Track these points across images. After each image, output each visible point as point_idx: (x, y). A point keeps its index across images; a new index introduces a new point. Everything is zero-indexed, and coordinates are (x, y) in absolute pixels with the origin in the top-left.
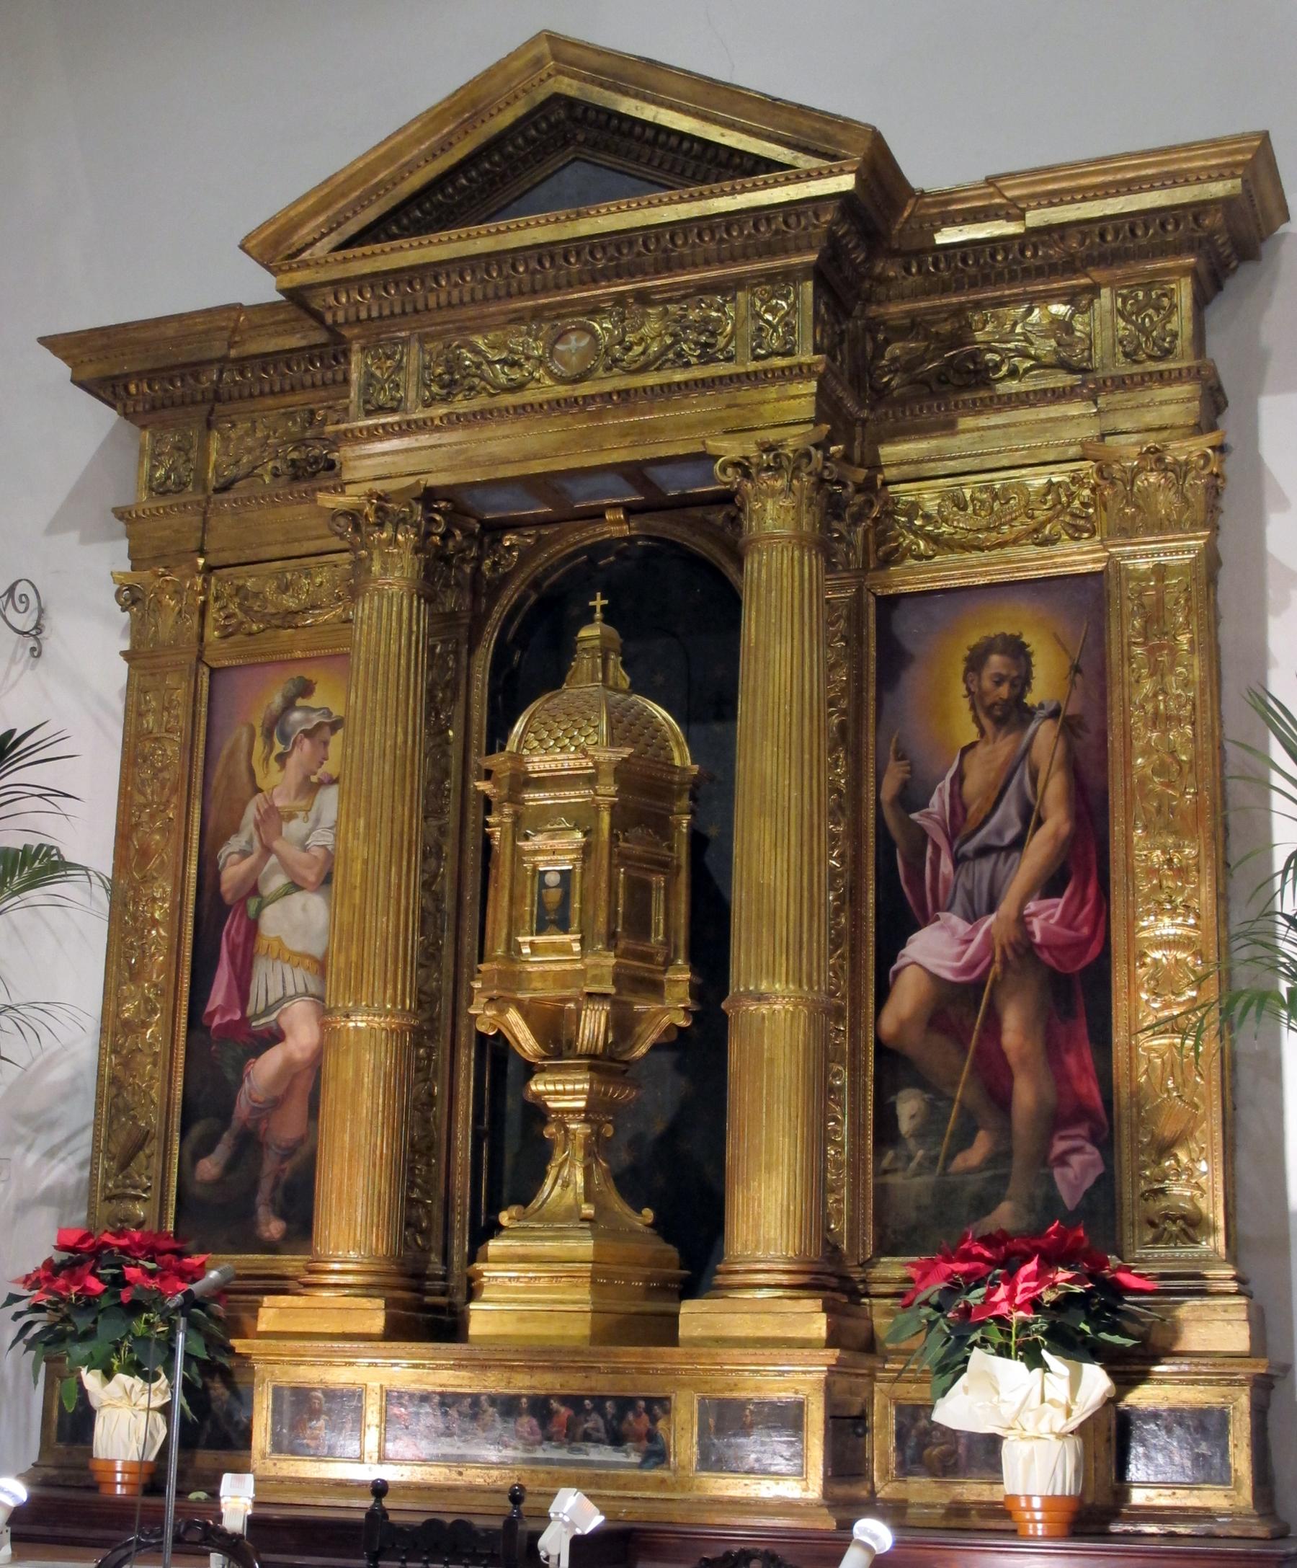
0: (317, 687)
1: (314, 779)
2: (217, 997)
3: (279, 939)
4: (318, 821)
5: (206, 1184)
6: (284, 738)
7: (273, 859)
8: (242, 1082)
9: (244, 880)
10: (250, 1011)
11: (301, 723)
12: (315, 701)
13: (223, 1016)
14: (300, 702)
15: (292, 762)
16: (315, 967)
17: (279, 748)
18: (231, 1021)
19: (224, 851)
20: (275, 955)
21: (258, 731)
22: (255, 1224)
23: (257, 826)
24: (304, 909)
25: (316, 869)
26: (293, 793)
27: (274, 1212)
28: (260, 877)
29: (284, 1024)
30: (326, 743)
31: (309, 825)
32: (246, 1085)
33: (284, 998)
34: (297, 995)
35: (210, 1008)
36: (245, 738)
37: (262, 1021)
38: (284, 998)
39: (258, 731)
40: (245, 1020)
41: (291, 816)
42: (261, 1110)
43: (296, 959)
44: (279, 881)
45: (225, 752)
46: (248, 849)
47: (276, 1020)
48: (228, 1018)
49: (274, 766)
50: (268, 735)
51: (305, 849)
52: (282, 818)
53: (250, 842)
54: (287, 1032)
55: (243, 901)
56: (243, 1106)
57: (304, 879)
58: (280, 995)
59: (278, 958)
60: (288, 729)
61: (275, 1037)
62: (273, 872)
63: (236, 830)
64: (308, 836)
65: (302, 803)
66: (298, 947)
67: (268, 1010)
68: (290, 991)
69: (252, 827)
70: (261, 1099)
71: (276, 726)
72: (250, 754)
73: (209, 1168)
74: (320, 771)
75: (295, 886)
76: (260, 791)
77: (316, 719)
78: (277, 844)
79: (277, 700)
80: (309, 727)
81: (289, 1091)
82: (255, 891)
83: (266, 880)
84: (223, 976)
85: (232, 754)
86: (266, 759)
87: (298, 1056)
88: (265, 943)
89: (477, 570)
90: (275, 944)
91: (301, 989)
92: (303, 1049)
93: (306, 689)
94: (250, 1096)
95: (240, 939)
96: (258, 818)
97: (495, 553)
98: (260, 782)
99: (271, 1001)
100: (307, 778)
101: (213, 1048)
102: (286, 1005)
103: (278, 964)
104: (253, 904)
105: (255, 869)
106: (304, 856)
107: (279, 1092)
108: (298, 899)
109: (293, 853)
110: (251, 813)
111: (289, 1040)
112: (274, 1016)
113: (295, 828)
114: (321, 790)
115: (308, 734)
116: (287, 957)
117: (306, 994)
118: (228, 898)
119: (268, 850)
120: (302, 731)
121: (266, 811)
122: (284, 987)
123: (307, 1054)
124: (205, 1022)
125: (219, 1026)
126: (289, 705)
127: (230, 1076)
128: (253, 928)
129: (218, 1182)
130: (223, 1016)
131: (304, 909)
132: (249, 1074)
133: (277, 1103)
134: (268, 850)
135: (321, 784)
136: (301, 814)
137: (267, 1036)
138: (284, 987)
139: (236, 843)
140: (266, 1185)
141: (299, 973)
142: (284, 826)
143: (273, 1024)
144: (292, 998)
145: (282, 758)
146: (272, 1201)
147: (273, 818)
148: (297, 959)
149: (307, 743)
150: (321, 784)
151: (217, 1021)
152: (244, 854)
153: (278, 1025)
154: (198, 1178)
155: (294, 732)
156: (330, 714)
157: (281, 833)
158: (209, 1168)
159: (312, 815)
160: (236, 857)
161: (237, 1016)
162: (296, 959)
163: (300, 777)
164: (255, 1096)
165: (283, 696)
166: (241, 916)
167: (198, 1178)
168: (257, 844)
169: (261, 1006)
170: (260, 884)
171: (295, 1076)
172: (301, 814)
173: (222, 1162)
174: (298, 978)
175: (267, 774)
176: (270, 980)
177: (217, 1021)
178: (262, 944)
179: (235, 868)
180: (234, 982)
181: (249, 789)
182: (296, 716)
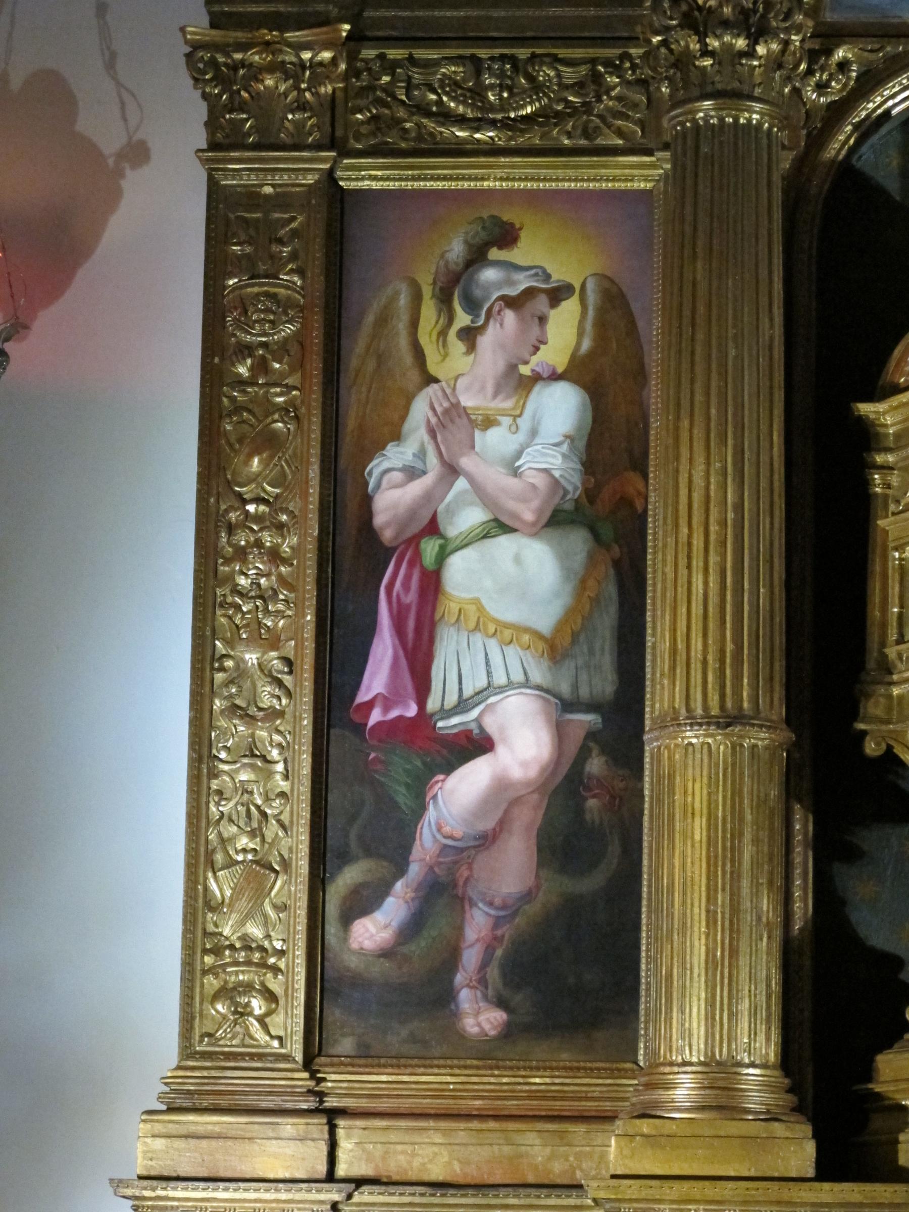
0: (523, 234)
1: (525, 370)
2: (376, 679)
3: (477, 602)
4: (534, 433)
5: (361, 953)
6: (472, 306)
7: (461, 484)
8: (423, 808)
9: (413, 513)
10: (432, 704)
11: (499, 285)
12: (517, 255)
13: (386, 709)
14: (494, 254)
15: (485, 341)
16: (541, 645)
17: (462, 319)
18: (400, 718)
19: (376, 467)
20: (472, 625)
21: (427, 292)
22: (456, 1015)
23: (432, 433)
24: (518, 559)
25: (536, 503)
26: (490, 389)
27: (485, 997)
28: (441, 508)
29: (491, 725)
30: (543, 320)
31: (521, 437)
32: (431, 814)
33: (490, 689)
34: (510, 685)
35: (363, 697)
36: (403, 301)
37: (455, 720)
38: (490, 689)
39: (427, 292)
40: (424, 719)
41: (489, 423)
42: (462, 850)
43: (507, 633)
44: (472, 517)
45: (370, 318)
46: (419, 465)
47: (477, 720)
48: (394, 714)
49: (457, 347)
50: (444, 299)
51: (516, 472)
52: (473, 424)
53: (421, 454)
54: (495, 736)
55: (414, 541)
56: (426, 842)
57: (516, 516)
58: (482, 682)
59: (477, 628)
60: (478, 293)
61: (476, 744)
62: (461, 502)
63: (397, 436)
64: (519, 455)
65: (508, 404)
66: (509, 616)
67: (463, 706)
68: (500, 679)
69: (422, 434)
70: (458, 833)
71: (455, 286)
72: (414, 324)
73: (372, 932)
74: (534, 359)
75: (500, 526)
76: (437, 381)
77: (523, 282)
78: (466, 462)
79: (456, 250)
80: (513, 292)
81: (503, 825)
82: (433, 528)
83: (451, 512)
84: (383, 651)
85: (383, 320)
86: (443, 334)
87: (517, 773)
88: (454, 607)
89: (796, 91)
90: (472, 609)
91: (518, 676)
92: (524, 764)
93: (506, 236)
94: (439, 829)
95: (411, 598)
96: (434, 420)
97: (823, 69)
98: (433, 368)
99: (468, 692)
100: (512, 368)
101: (372, 755)
102: (492, 700)
103: (478, 639)
104: (430, 548)
105: (429, 497)
106: (512, 483)
107: (488, 824)
108: (505, 544)
109: (496, 478)
110: (420, 410)
111: (500, 749)
112: (475, 713)
113: (496, 441)
114: (537, 388)
115: (511, 302)
116: (492, 628)
117: (527, 684)
118: (387, 535)
119: (452, 471)
120: (503, 298)
121: (446, 412)
122: (489, 674)
123: (533, 772)
124: (356, 718)
125: (379, 724)
126: (477, 257)
127: (403, 797)
128: (432, 583)
129: (386, 953)
130: (386, 709)
131: (518, 559)
132: (435, 797)
133: (486, 841)
134: (452, 471)
135: (536, 378)
136: (506, 421)
137: (464, 742)
138: (489, 674)
139: (395, 456)
140: (471, 958)
141: (513, 653)
142: (477, 433)
143: (473, 726)
144: (501, 689)
145: (470, 336)
146: (483, 982)
147: (455, 422)
148: (510, 633)
149: (509, 316)
150: (536, 378)
151: (376, 716)
152: (412, 473)
153: (481, 728)
154: (354, 945)
155: (486, 298)
156: (547, 277)
157: (473, 447)
158: (372, 932)
159: (524, 423)
160: (397, 476)
161: (412, 711)
162: (507, 633)
163: (501, 365)
164: (447, 829)
165: (466, 242)
166: (411, 564)
167: (354, 945)
168: (432, 460)
169: (452, 699)
170: (440, 519)
171: (515, 802)
172: (506, 421)
173: (395, 924)
174: (511, 662)
175: (445, 356)
176: (461, 663)
177: (376, 716)
178: (448, 607)
179: (396, 494)
180: (403, 662)
181: (414, 376)
182: (489, 275)
